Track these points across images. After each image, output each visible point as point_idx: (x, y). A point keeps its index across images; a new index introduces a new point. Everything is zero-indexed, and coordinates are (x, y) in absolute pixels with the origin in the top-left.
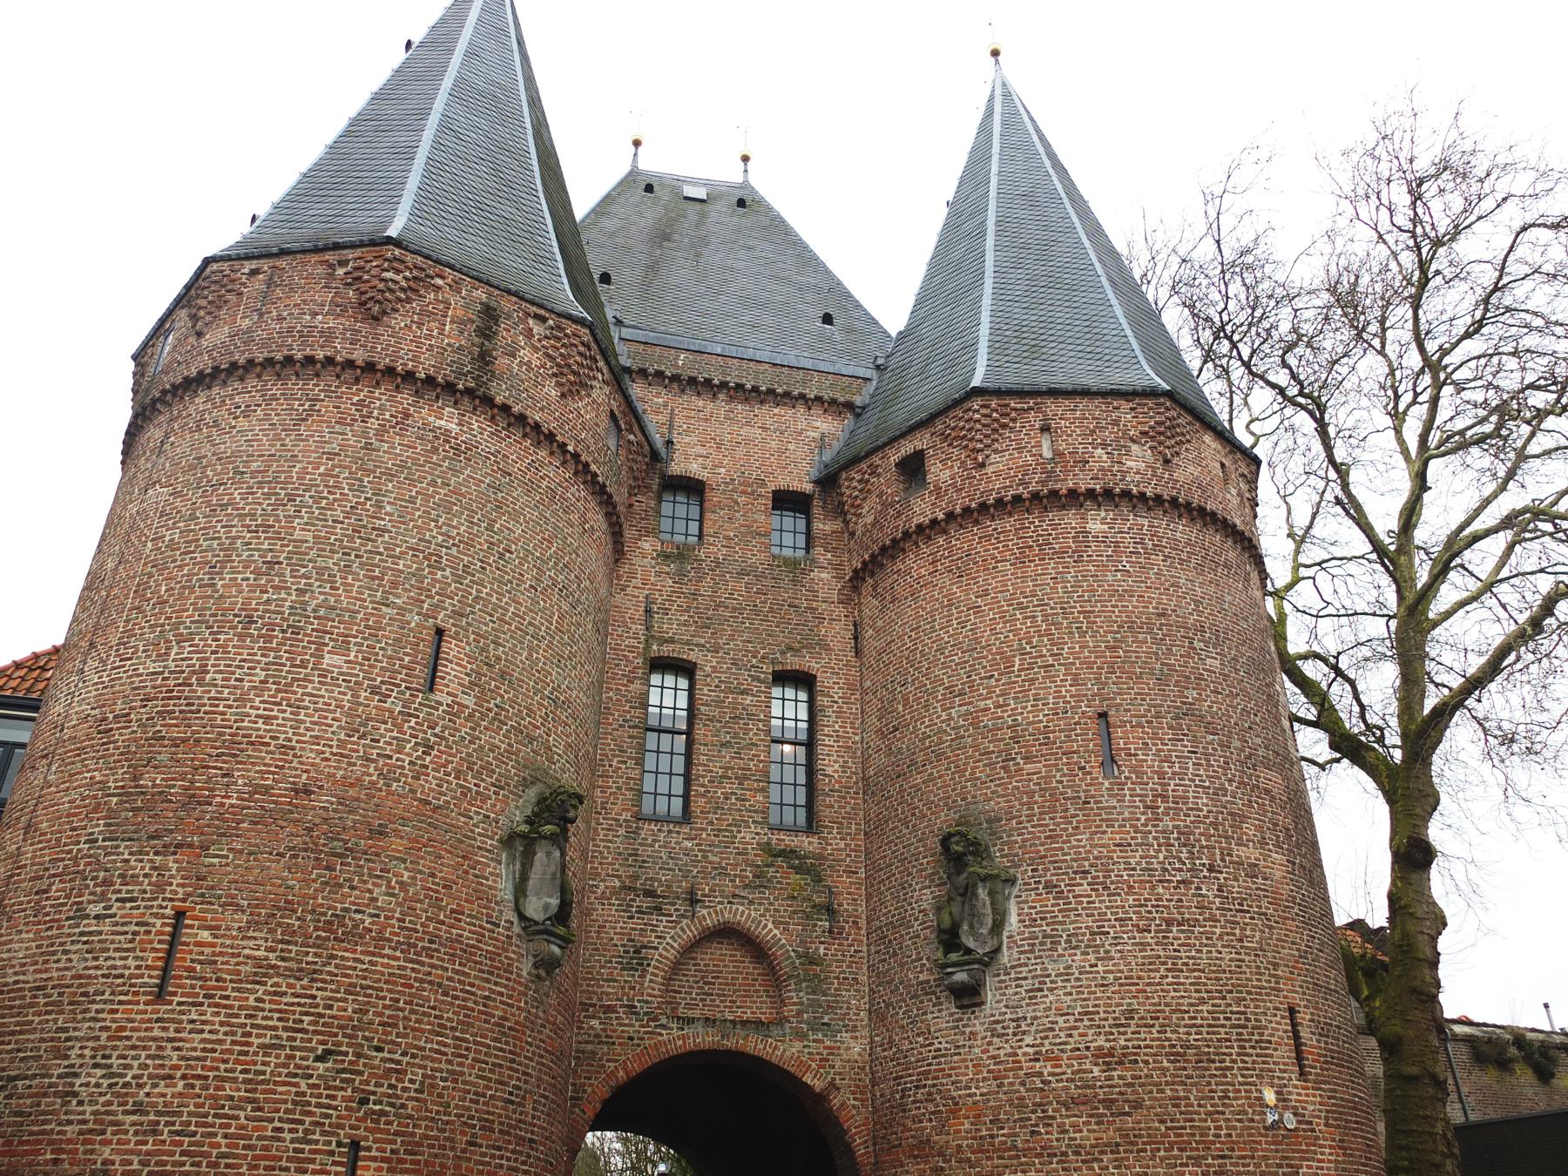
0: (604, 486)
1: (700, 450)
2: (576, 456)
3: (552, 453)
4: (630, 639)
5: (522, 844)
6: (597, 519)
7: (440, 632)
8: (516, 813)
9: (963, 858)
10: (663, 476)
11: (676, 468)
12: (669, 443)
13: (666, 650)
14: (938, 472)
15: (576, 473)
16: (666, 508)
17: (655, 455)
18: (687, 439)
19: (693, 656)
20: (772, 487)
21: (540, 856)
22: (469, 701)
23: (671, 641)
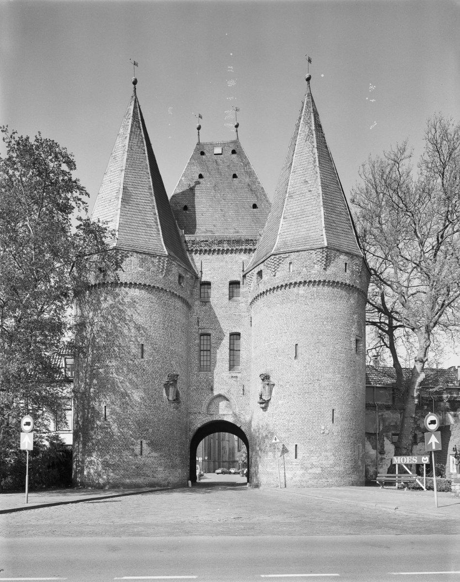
0: (179, 296)
1: (209, 272)
2: (170, 291)
3: (164, 293)
4: (195, 329)
5: (167, 386)
6: (179, 304)
7: (143, 345)
8: (166, 379)
9: (266, 378)
10: (201, 281)
11: (203, 279)
12: (201, 272)
13: (203, 331)
14: (265, 277)
15: (171, 295)
16: (202, 290)
17: (197, 278)
18: (205, 270)
19: (210, 332)
20: (229, 280)
21: (171, 388)
22: (151, 359)
23: (204, 328)
